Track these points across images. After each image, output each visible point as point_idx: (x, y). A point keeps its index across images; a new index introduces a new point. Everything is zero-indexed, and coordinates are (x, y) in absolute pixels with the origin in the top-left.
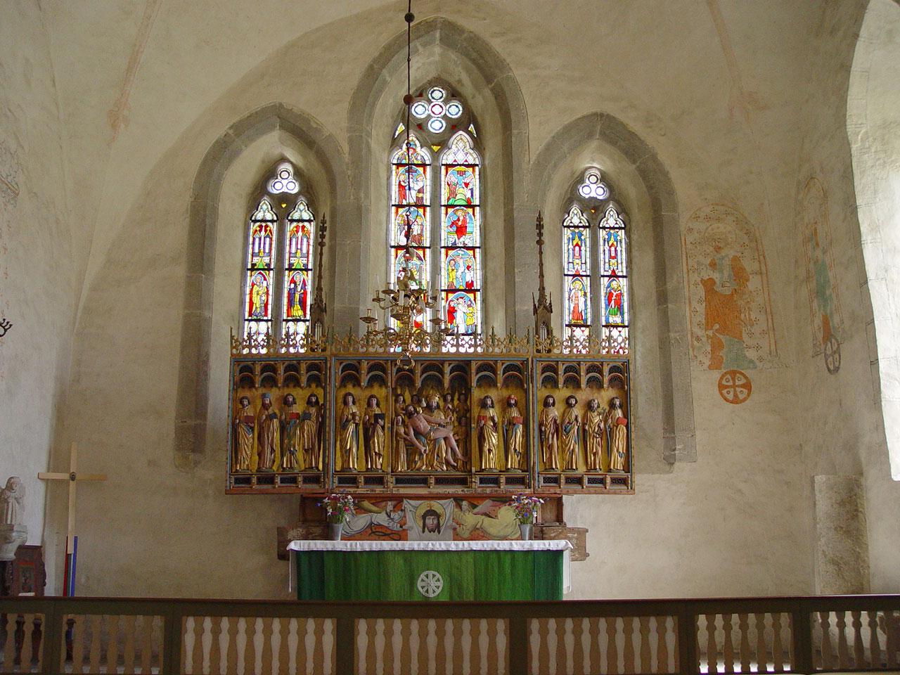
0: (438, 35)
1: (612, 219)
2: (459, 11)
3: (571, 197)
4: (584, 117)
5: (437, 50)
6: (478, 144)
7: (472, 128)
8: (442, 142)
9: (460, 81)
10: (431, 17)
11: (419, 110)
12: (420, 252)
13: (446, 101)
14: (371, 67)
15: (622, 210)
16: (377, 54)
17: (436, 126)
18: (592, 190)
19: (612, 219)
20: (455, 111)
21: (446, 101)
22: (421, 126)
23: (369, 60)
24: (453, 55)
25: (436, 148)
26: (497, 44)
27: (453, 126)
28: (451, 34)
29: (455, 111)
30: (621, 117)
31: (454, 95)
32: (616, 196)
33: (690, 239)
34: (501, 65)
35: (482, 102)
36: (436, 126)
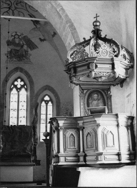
1: (50, 104)
3: (43, 100)
6: (26, 90)
7: (25, 87)
8: (20, 89)
11: (16, 83)
12: (15, 110)
13: (21, 82)
15: (52, 102)
17: (19, 86)
18: (47, 98)
19: (50, 104)
20: (22, 83)
21: (21, 82)
22: (15, 86)
25: (19, 90)
27: (22, 86)
28: (21, 70)
29: (22, 83)
31: (22, 80)
32: (51, 100)
33: (62, 109)
35: (28, 82)
36: (19, 86)
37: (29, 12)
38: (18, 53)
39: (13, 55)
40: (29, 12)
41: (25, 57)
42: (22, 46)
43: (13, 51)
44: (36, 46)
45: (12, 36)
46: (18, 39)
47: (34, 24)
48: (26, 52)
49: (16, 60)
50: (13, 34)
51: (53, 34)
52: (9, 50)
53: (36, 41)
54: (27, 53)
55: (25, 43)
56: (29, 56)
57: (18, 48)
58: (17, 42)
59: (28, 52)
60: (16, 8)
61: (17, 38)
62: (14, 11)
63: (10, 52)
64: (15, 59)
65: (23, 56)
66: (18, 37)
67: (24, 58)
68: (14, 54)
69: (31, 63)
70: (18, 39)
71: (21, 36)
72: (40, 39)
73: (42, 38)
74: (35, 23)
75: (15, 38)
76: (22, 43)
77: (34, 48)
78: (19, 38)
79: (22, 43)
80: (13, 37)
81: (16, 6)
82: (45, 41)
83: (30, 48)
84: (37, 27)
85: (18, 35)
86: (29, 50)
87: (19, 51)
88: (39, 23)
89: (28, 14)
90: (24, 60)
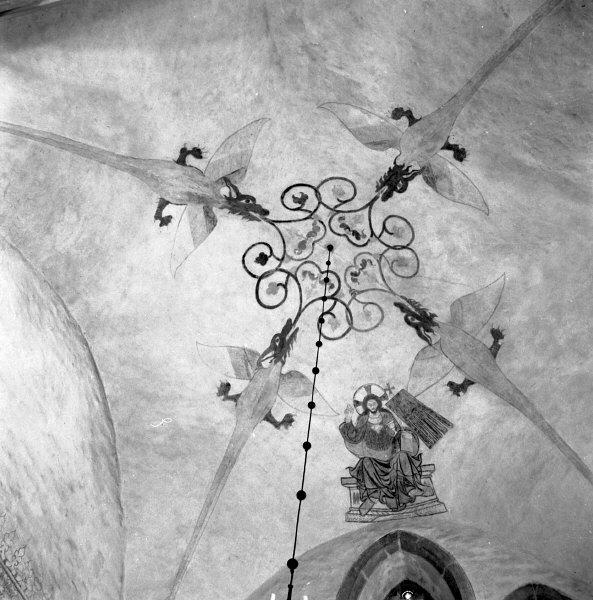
0: (399, 543)
2: (413, 525)
4: (520, 589)
5: (400, 554)
9: (422, 580)
10: (393, 531)
14: (352, 569)
16: (356, 560)
23: (350, 565)
24: (413, 558)
26: (441, 543)
28: (409, 543)
30: (551, 585)
34: (447, 556)
37: (395, 294)
38: (387, 474)
39: (369, 485)
40: (395, 294)
41: (414, 487)
42: (396, 440)
43: (367, 464)
44: (444, 421)
45: (357, 403)
46: (378, 413)
47: (420, 335)
48: (415, 459)
49: (385, 506)
50: (360, 397)
51: (489, 341)
52: (354, 461)
53: (435, 398)
54: (417, 463)
55: (403, 425)
56: (430, 477)
57: (383, 455)
58: (377, 428)
59: (419, 457)
60: (354, 293)
61: (374, 413)
62: (350, 307)
63: (359, 473)
64: (378, 505)
65: (406, 483)
66: (377, 405)
67: (412, 493)
68: (372, 480)
69: (442, 508)
70: (378, 413)
71: (384, 397)
72: (451, 384)
73: (459, 380)
74: (422, 329)
75: (367, 412)
76: (392, 426)
77: (438, 435)
78: (380, 408)
79: (392, 426)
80: (361, 409)
81: (355, 286)
82: (471, 389)
83: (426, 441)
84: (430, 345)
85: (374, 397)
86: (423, 447)
87: (387, 466)
88: (435, 324)
89: (396, 304)
90: (412, 500)
